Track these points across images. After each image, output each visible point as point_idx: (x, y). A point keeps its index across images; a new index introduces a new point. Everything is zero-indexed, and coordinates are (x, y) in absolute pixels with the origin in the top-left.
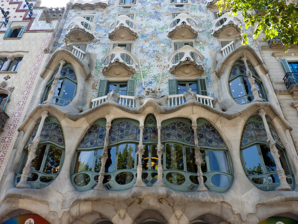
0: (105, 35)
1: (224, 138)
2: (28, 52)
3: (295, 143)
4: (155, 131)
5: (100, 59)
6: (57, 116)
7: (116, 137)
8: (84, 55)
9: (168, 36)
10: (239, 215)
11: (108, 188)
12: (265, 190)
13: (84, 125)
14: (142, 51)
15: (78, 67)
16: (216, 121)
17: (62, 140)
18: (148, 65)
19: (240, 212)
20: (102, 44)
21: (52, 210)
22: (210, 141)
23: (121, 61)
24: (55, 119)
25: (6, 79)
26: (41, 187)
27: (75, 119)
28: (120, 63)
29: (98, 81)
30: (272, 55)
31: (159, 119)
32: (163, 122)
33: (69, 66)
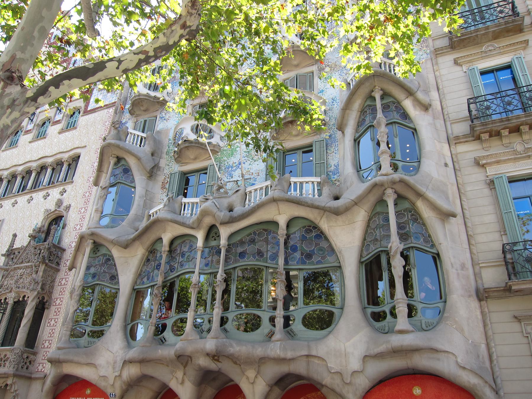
1: (335, 248)
2: (86, 146)
3: (469, 237)
8: (145, 138)
10: (339, 373)
11: (163, 341)
12: (383, 331)
13: (139, 252)
15: (134, 162)
16: (319, 219)
17: (114, 278)
19: (341, 369)
21: (102, 374)
24: (105, 248)
25: (62, 193)
26: (90, 345)
27: (126, 246)
28: (190, 142)
30: (455, 63)
31: (224, 232)
32: (231, 236)
33: (123, 162)
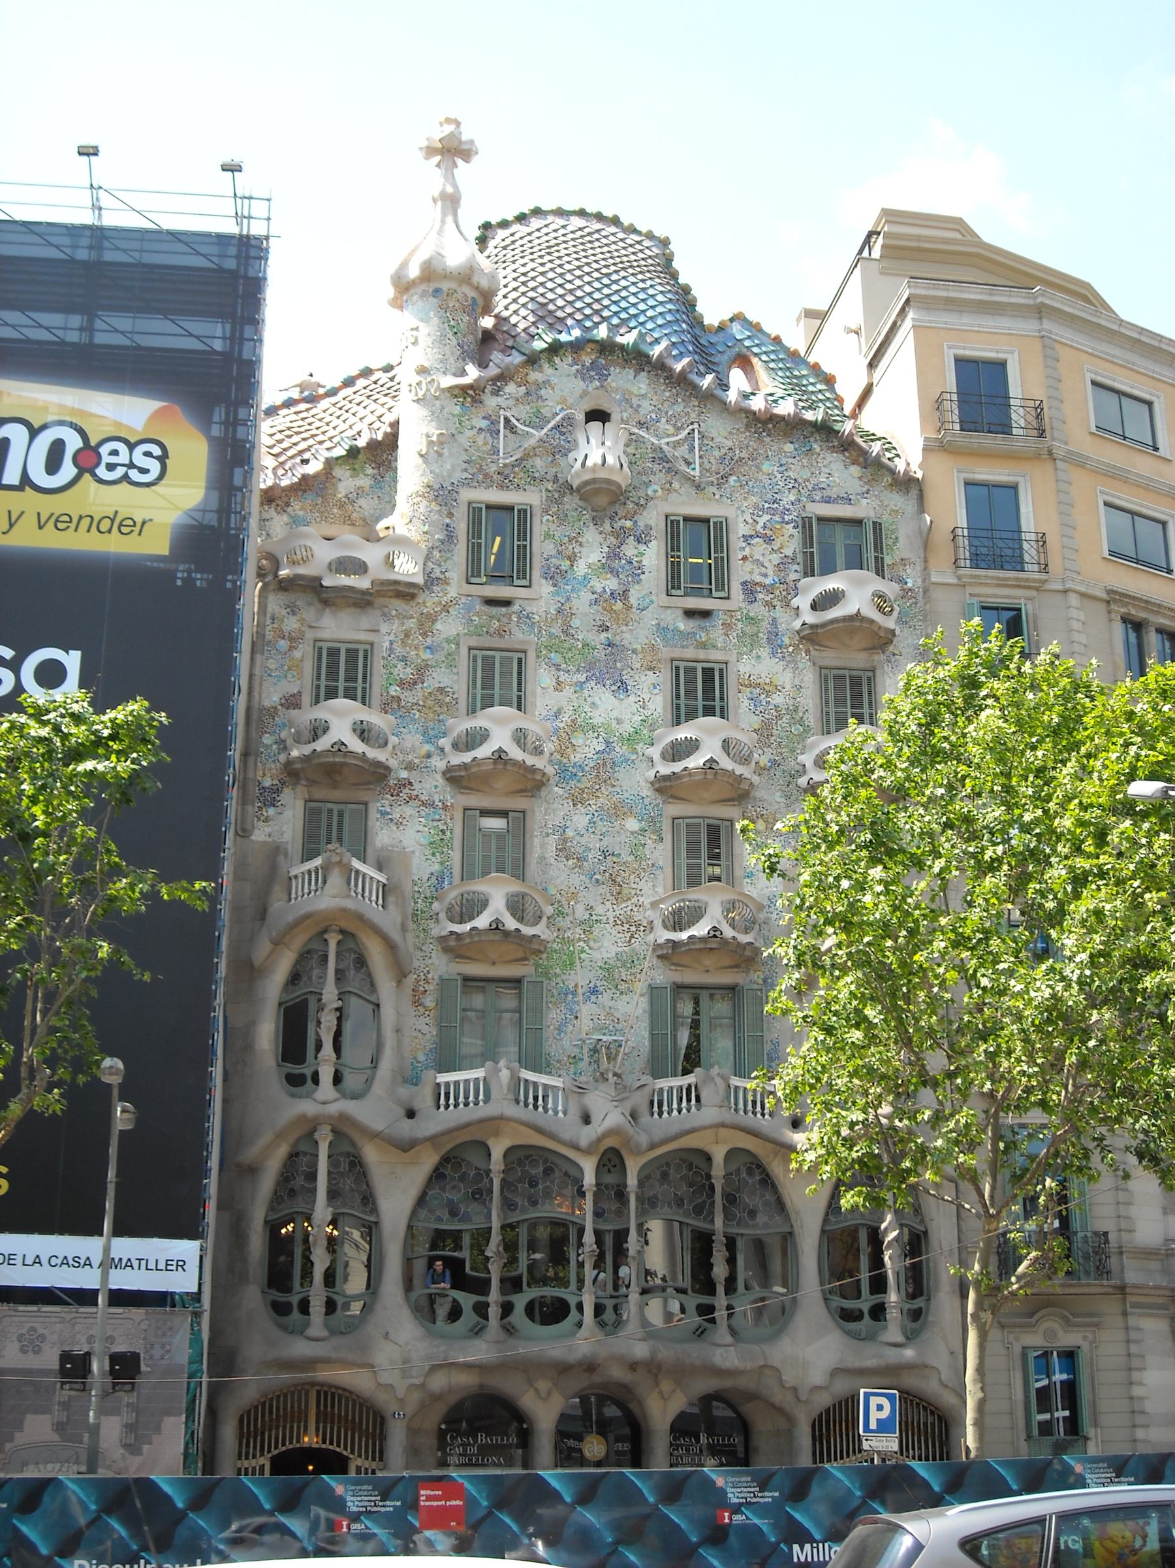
0: (429, 756)
1: (788, 1204)
4: (621, 1194)
5: (425, 880)
6: (356, 1136)
7: (519, 1200)
8: (384, 885)
9: (652, 783)
10: (795, 1390)
14: (563, 849)
18: (587, 917)
20: (424, 804)
22: (752, 1214)
23: (511, 924)
28: (507, 934)
29: (428, 972)
